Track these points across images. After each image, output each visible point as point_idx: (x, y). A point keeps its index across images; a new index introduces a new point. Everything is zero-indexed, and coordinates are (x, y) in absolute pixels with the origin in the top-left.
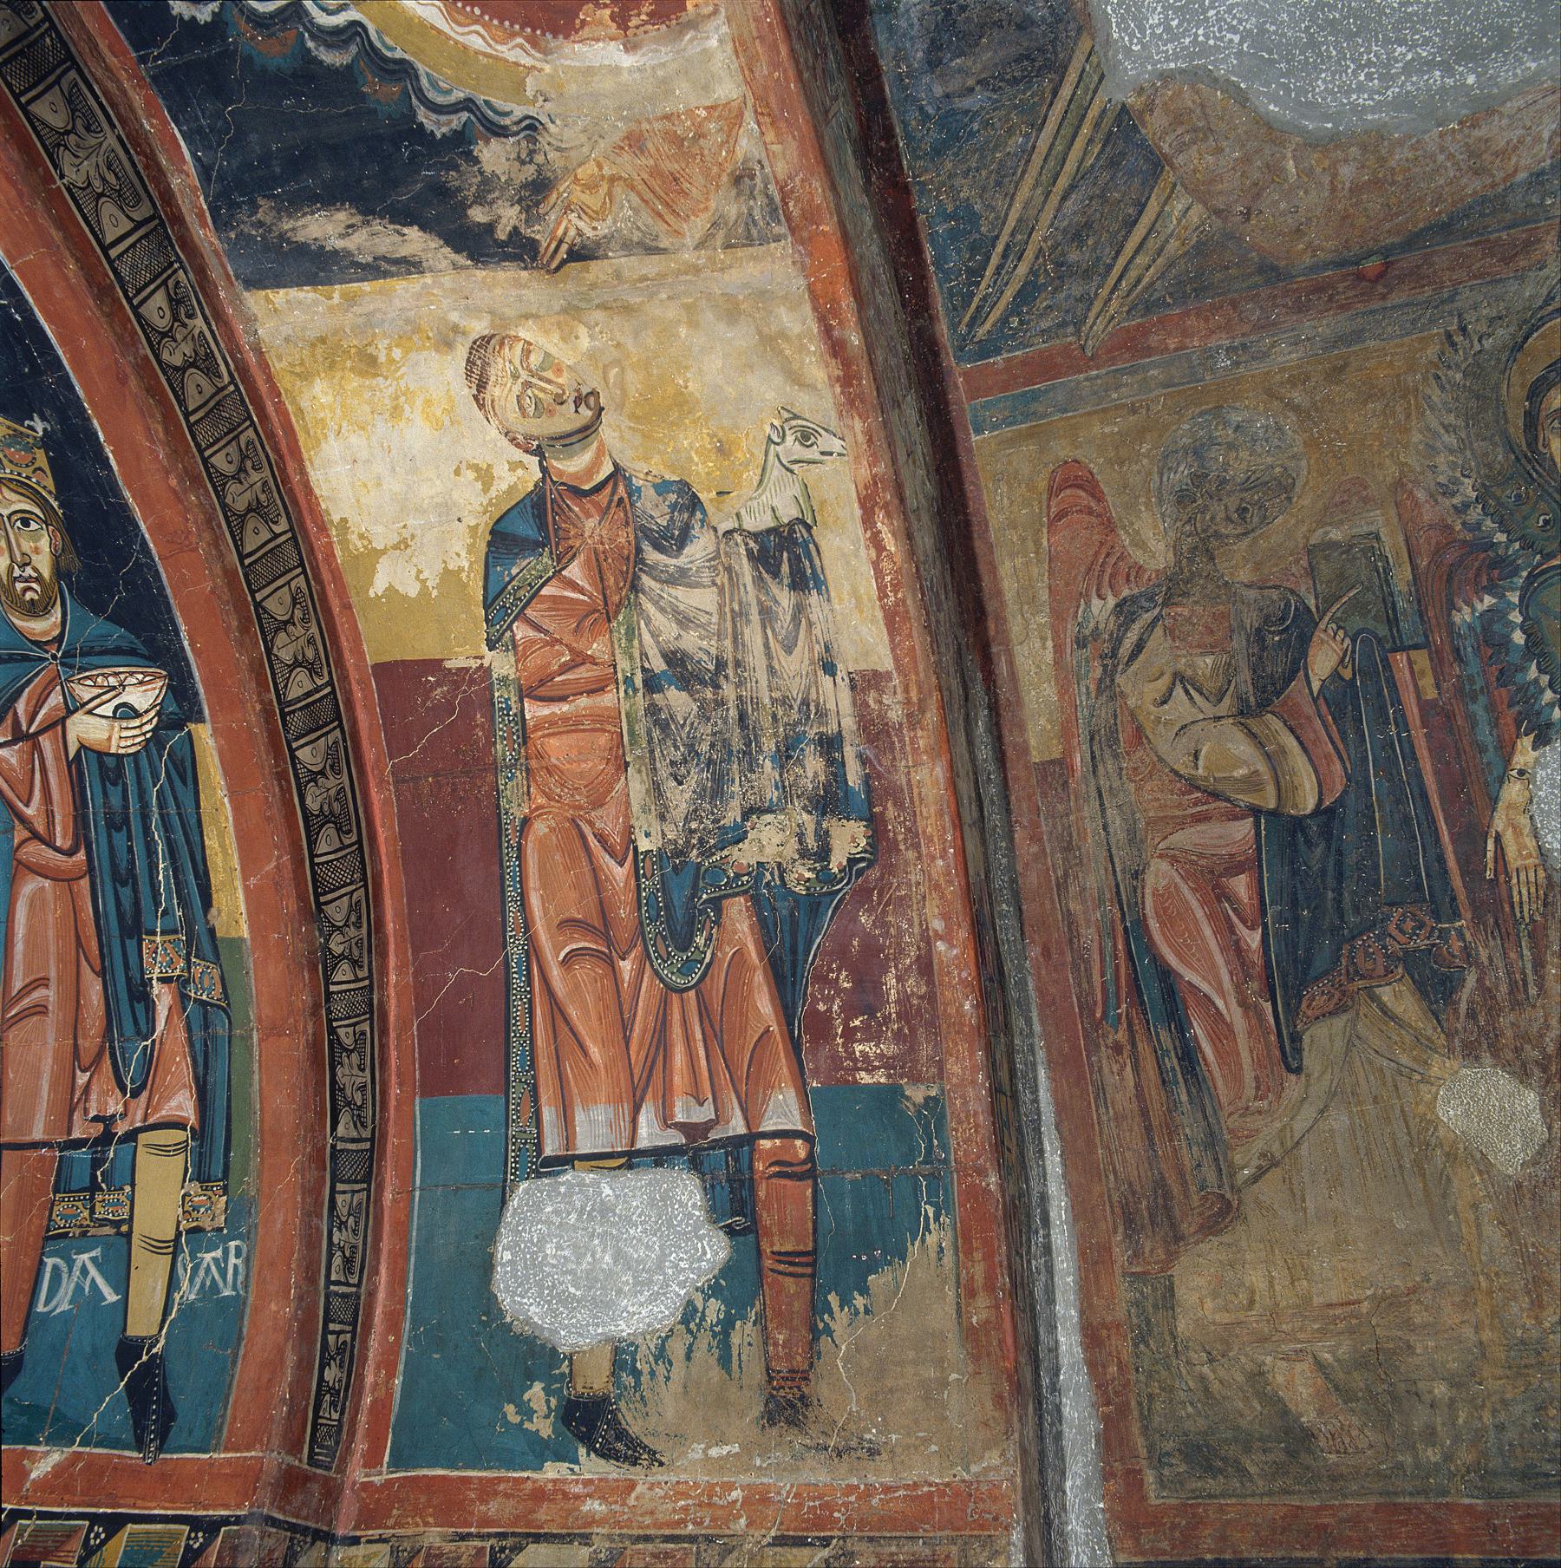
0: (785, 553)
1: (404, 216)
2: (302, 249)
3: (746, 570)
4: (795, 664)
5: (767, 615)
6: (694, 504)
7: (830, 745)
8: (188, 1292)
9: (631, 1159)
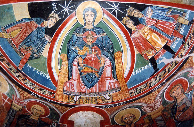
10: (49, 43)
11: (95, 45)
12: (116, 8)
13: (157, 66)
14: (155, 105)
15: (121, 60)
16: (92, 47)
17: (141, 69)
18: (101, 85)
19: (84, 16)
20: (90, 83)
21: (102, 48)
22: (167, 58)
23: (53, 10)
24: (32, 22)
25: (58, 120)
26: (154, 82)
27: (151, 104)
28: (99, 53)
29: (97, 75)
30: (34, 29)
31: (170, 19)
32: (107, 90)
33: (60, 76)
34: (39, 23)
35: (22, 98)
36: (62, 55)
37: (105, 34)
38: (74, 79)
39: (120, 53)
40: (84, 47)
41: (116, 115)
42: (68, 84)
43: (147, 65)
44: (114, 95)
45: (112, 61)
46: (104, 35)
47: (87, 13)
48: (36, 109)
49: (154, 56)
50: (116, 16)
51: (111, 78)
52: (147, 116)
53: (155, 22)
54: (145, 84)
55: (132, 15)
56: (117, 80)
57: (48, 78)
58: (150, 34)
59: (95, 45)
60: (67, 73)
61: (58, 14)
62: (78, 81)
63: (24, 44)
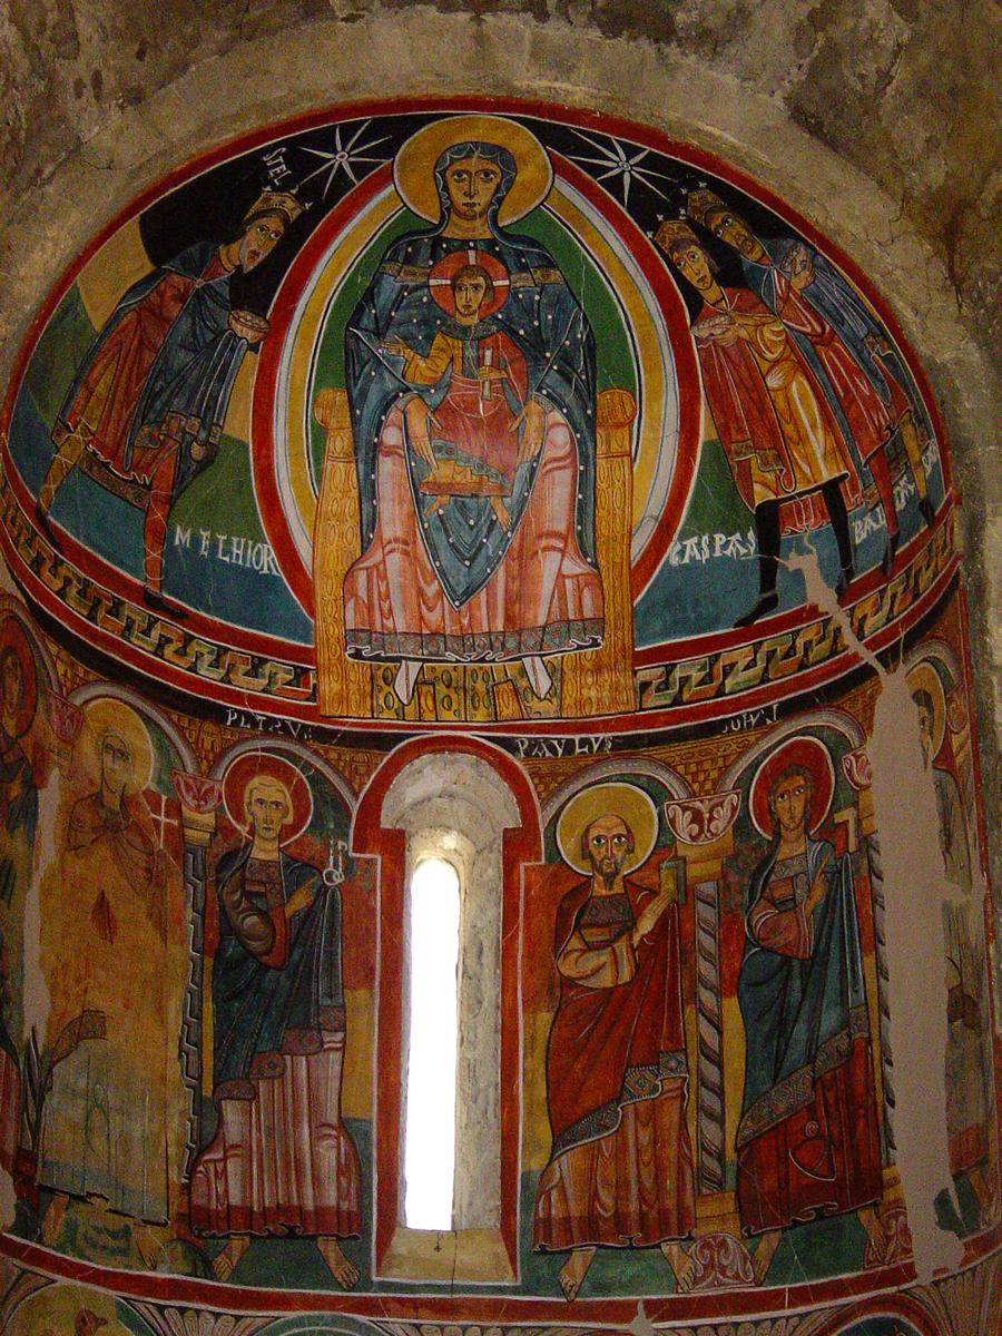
10: (253, 348)
11: (495, 328)
12: (627, 167)
13: (779, 577)
14: (711, 812)
15: (626, 443)
16: (480, 339)
17: (711, 545)
18: (517, 583)
19: (444, 177)
20: (467, 563)
21: (533, 348)
22: (820, 562)
23: (266, 179)
24: (163, 286)
25: (345, 836)
26: (742, 667)
27: (701, 801)
28: (519, 379)
29: (502, 516)
30: (174, 310)
31: (874, 375)
32: (541, 621)
33: (320, 540)
34: (194, 269)
35: (204, 766)
36: (320, 400)
37: (555, 275)
38: (390, 542)
39: (626, 397)
40: (438, 340)
41: (564, 813)
42: (362, 578)
43: (738, 536)
44: (569, 675)
45: (582, 433)
46: (553, 278)
47: (458, 166)
48: (261, 801)
49: (774, 501)
50: (621, 201)
51: (566, 545)
52: (676, 858)
53: (819, 330)
54: (703, 658)
55: (713, 227)
56: (595, 565)
57: (269, 568)
58: (786, 365)
59: (495, 328)
60: (351, 506)
61: (294, 192)
62: (406, 553)
63: (142, 424)
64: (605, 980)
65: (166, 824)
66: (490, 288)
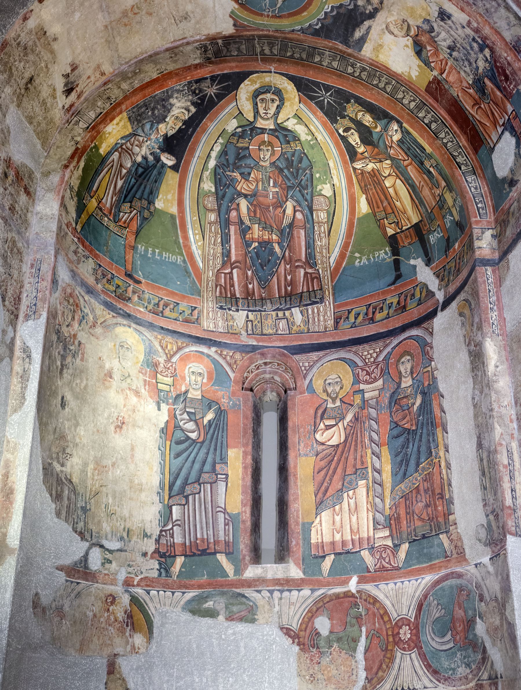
0: (444, 15)
1: (362, 22)
2: (359, 40)
3: (442, 23)
4: (460, 31)
5: (450, 27)
6: (428, 21)
7: (474, 39)
8: (458, 209)
9: (500, 138)
64: (334, 441)
65: (149, 381)
66: (273, 152)
